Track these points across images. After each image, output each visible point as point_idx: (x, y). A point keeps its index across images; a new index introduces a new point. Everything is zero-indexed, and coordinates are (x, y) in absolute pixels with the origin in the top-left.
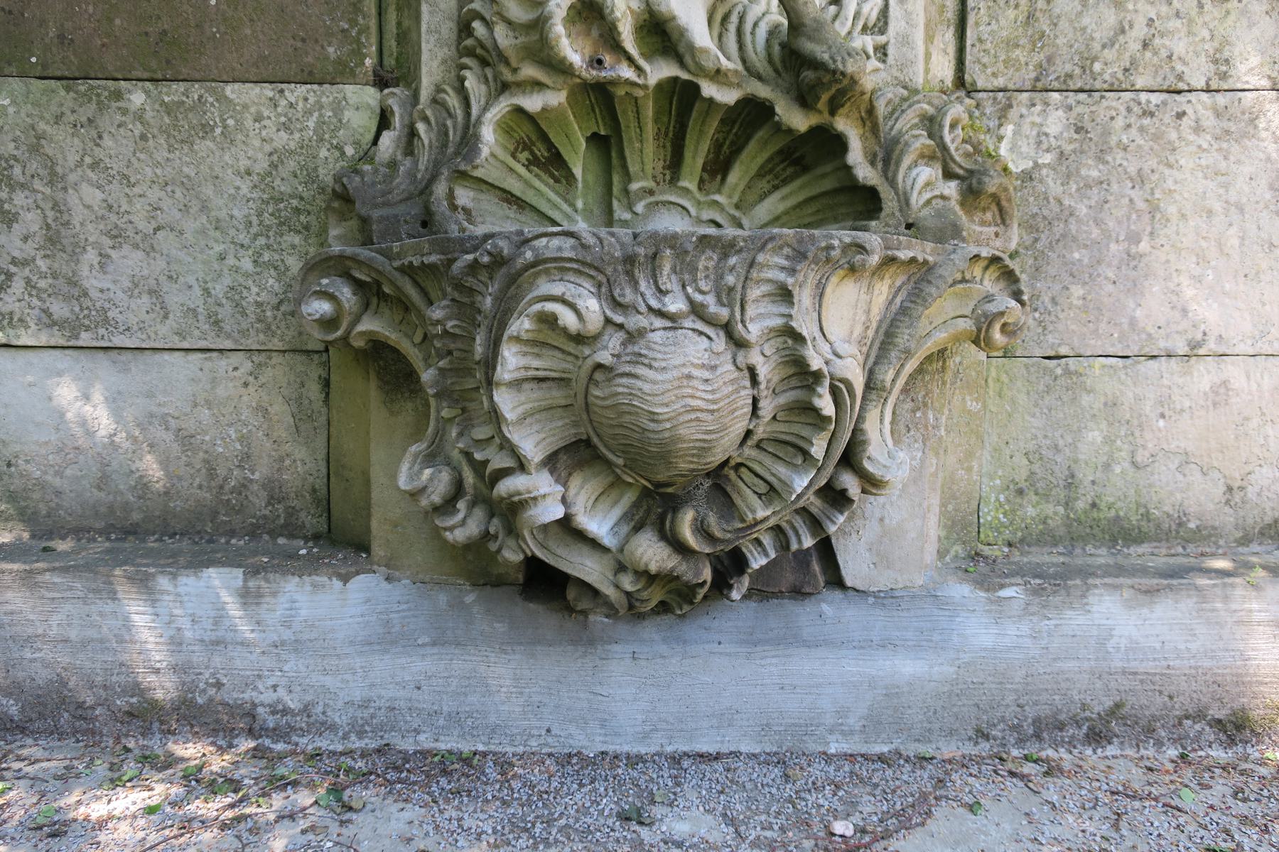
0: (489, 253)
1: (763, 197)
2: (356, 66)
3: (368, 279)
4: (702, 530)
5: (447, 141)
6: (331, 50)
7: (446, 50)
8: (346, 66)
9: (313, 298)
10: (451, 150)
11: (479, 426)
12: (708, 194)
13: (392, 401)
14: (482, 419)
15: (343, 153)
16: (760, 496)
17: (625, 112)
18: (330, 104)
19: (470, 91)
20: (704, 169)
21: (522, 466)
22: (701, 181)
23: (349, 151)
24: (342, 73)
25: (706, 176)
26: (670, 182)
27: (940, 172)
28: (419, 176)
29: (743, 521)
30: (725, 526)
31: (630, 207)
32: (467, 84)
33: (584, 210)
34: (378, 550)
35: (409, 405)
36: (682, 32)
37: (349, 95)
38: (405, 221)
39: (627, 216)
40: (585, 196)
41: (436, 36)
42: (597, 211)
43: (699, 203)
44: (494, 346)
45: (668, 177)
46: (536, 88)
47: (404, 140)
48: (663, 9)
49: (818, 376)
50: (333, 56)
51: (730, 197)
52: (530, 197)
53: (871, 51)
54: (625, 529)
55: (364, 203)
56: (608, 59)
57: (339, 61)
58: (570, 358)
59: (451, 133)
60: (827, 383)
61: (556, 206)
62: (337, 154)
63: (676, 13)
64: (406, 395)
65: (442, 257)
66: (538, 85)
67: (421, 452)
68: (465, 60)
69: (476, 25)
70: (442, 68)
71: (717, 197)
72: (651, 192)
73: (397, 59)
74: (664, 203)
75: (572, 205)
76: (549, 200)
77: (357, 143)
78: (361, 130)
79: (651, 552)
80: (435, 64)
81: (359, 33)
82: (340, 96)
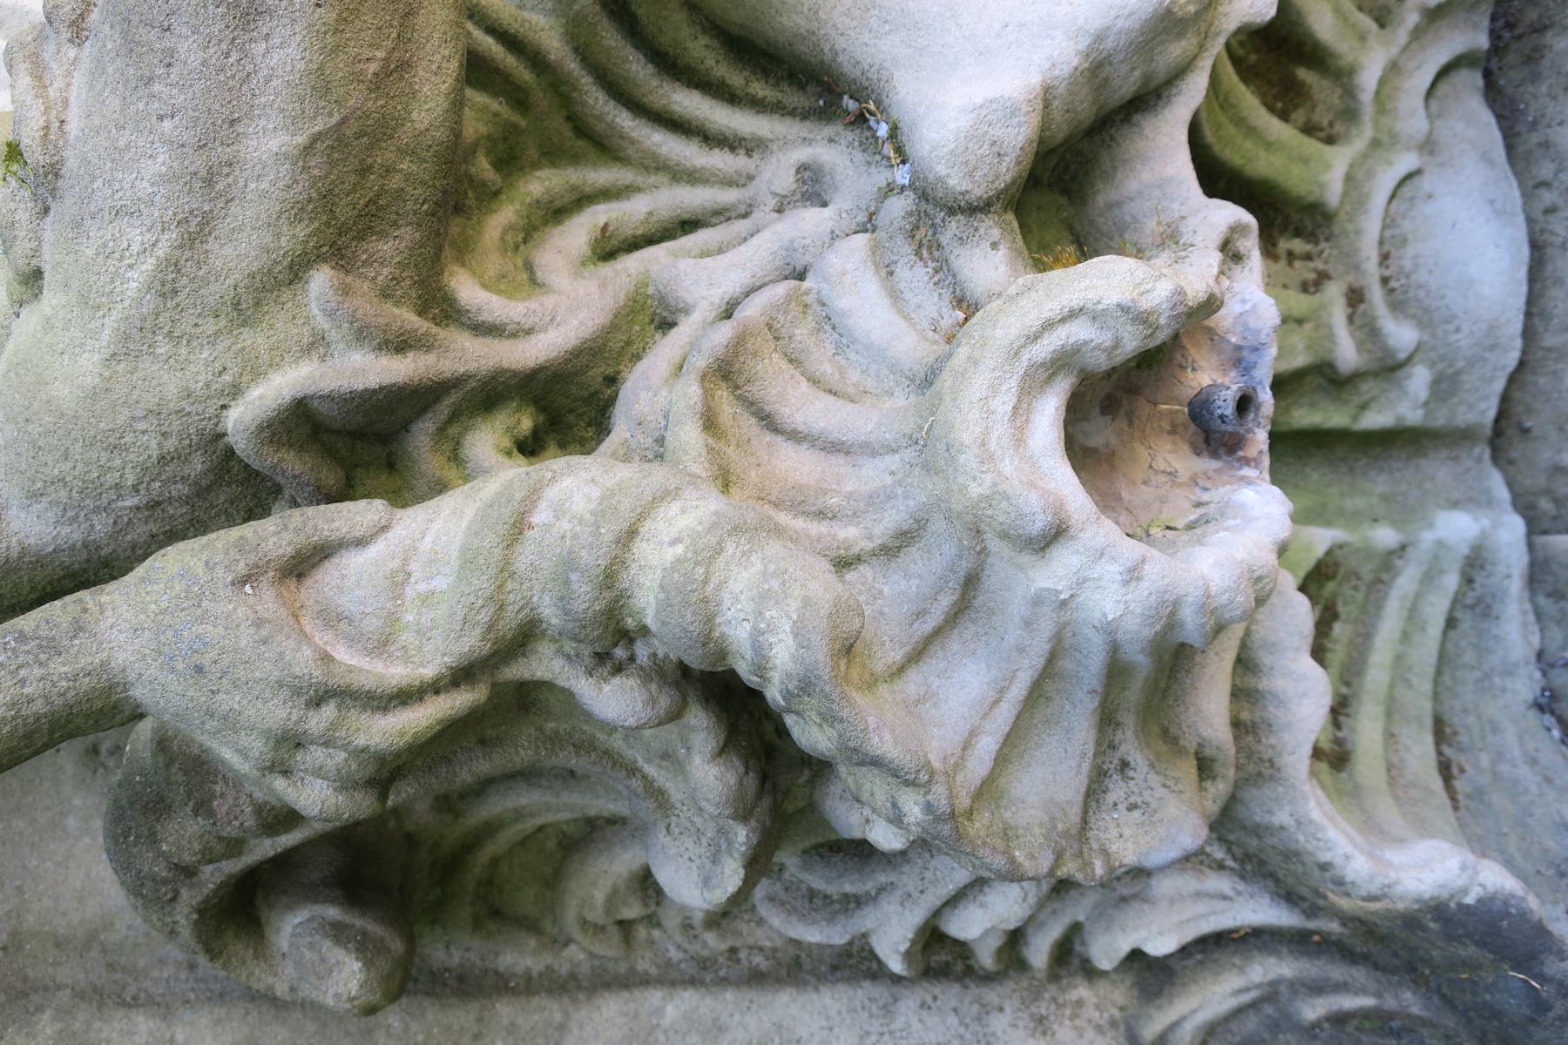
5: (1364, 1014)
7: (998, 1022)
10: (1410, 1001)
12: (1350, 114)
19: (1189, 934)
20: (1284, 116)
22: (1309, 130)
25: (1299, 116)
26: (1312, 238)
31: (1390, 368)
32: (1161, 945)
33: (1394, 524)
36: (1096, 69)
39: (1419, 379)
42: (1380, 484)
43: (1375, 143)
45: (1298, 245)
48: (1018, 136)
52: (1420, 701)
56: (1205, 375)
59: (1349, 1003)
61: (1413, 614)
63: (1035, 80)
68: (1039, 952)
71: (1369, 78)
72: (1355, 297)
74: (1385, 258)
75: (1389, 562)
76: (1405, 636)
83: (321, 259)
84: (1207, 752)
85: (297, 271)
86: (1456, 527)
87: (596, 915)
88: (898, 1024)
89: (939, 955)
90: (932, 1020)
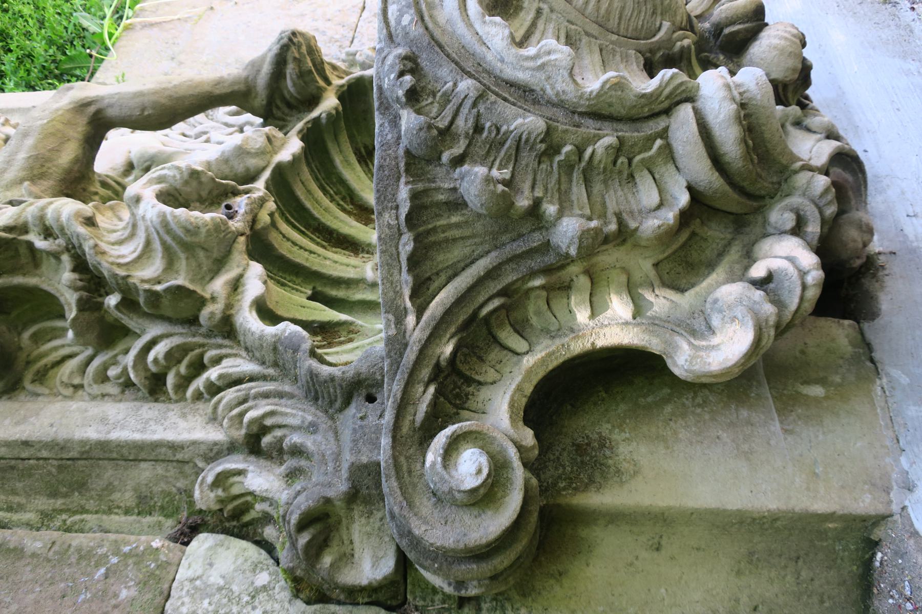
0: (401, 74)
2: (156, 560)
3: (432, 389)
6: (124, 594)
7: (170, 414)
8: (152, 574)
9: (454, 473)
11: (639, 202)
13: (618, 471)
14: (630, 196)
15: (264, 588)
17: (290, 252)
18: (193, 601)
23: (263, 578)
24: (160, 580)
28: (310, 418)
34: (864, 504)
35: (623, 450)
37: (190, 574)
38: (361, 418)
41: (151, 423)
44: (525, 94)
45: (366, 256)
46: (239, 290)
47: (262, 462)
50: (133, 592)
55: (330, 485)
57: (143, 584)
58: (540, 25)
62: (262, 596)
64: (608, 453)
65: (403, 180)
66: (236, 285)
67: (690, 344)
70: (189, 417)
73: (167, 516)
77: (256, 568)
78: (240, 561)
80: (182, 424)
81: (117, 553)
82: (187, 586)
83: (28, 180)
84: (215, 295)
85: (21, 181)
87: (65, 379)
88: (140, 412)
90: (150, 412)
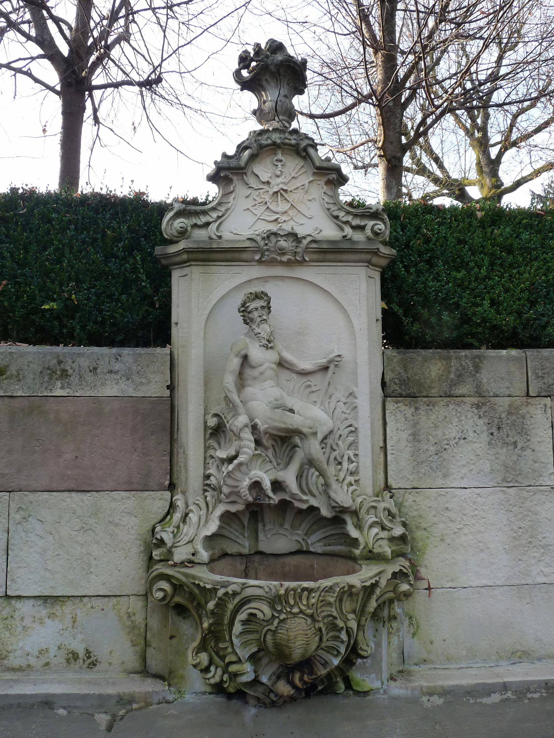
1: (315, 532)
4: (301, 679)
16: (322, 665)
21: (239, 661)
27: (380, 528)
29: (316, 675)
30: (310, 677)
40: (248, 532)
49: (342, 628)
51: (303, 531)
53: (353, 482)
54: (274, 678)
60: (345, 630)
69: (212, 478)
79: (284, 688)
86: (247, 545)
89: (208, 477)
